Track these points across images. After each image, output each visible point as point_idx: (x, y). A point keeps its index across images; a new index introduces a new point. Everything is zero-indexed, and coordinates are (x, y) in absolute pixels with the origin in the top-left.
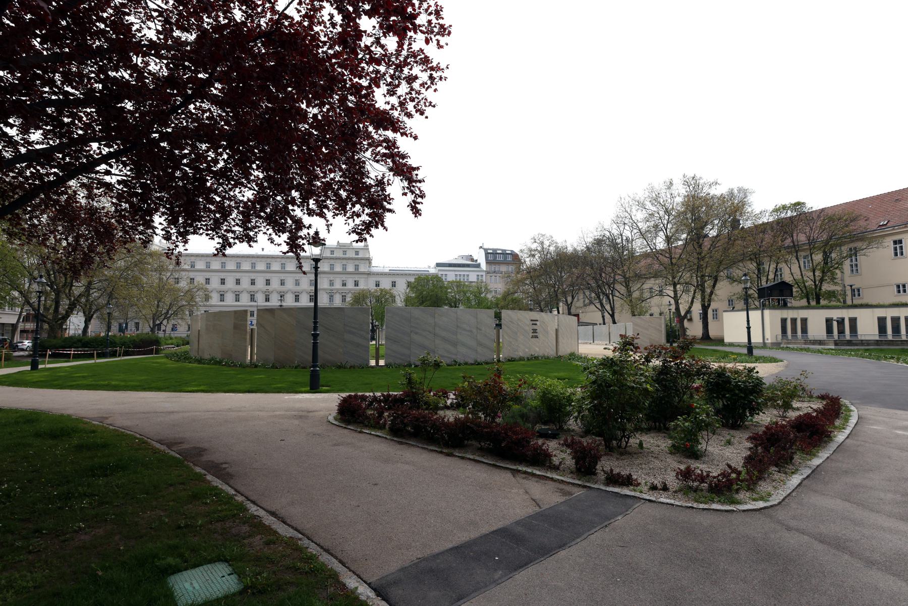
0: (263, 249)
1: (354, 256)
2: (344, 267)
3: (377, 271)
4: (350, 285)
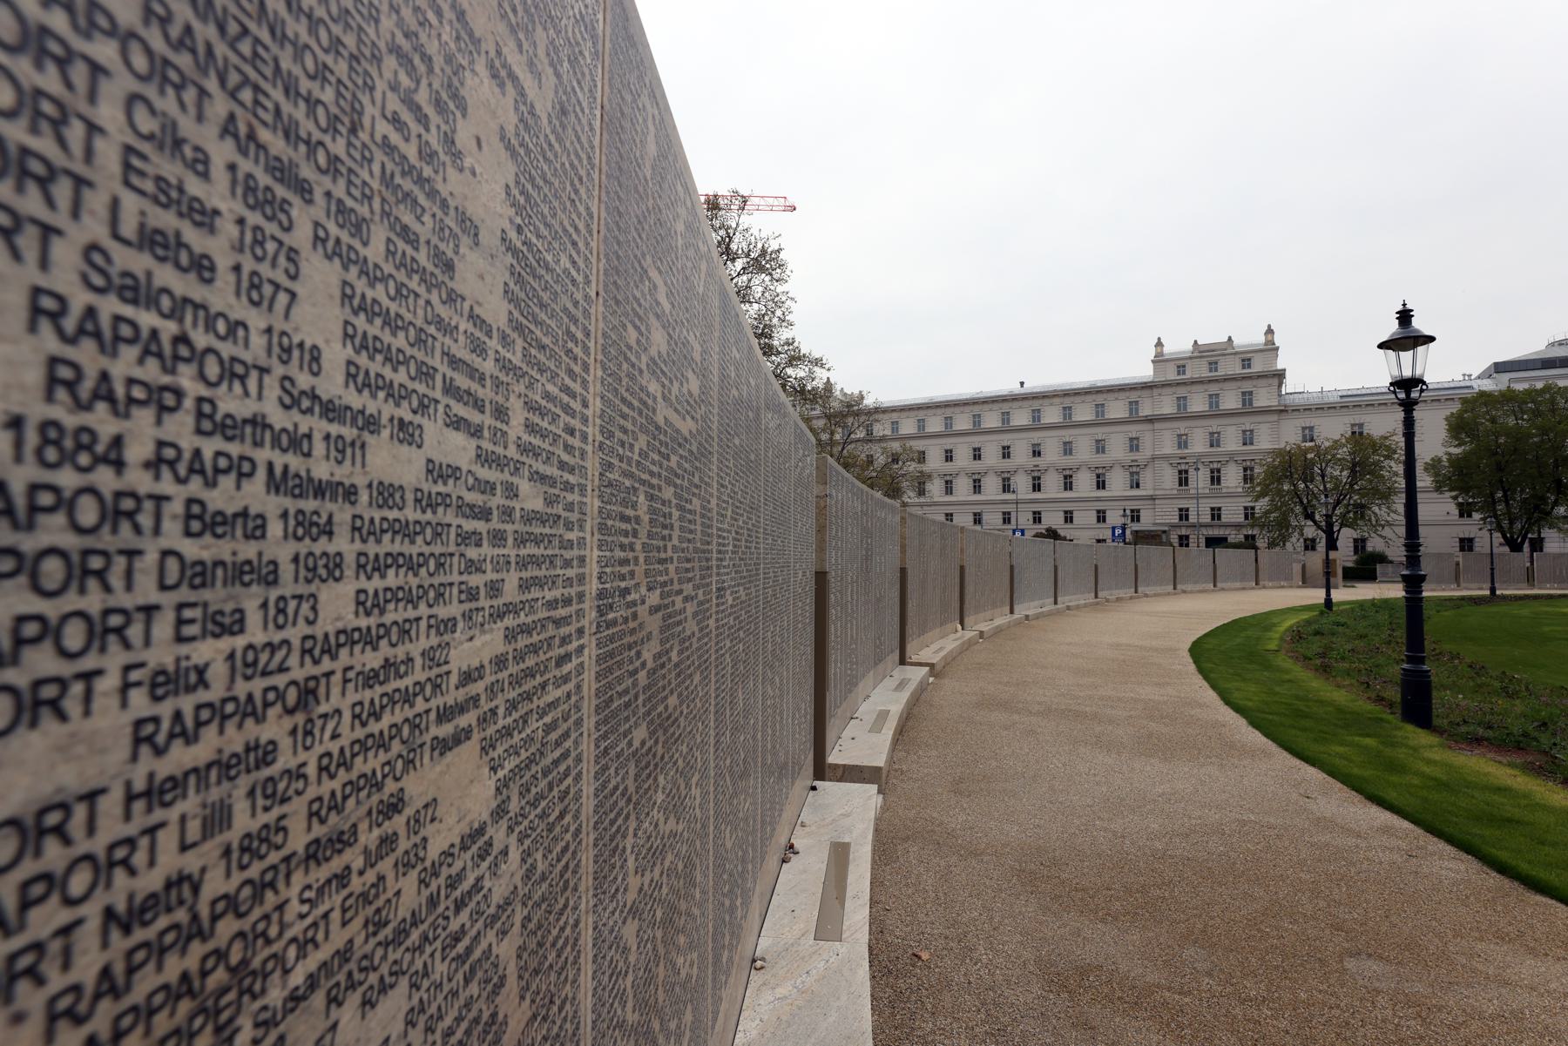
0: (1022, 384)
1: (1237, 369)
2: (1214, 399)
3: (1302, 402)
4: (1232, 442)
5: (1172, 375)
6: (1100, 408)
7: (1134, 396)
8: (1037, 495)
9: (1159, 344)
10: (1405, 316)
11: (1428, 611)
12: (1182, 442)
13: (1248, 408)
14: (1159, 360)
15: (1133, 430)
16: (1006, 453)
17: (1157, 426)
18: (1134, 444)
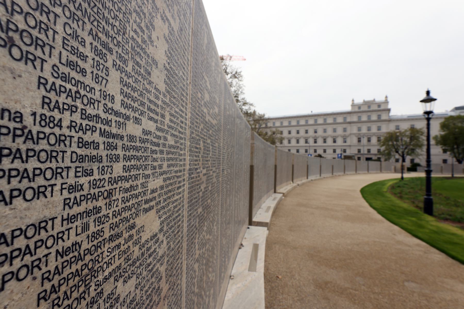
0: (312, 112)
2: (369, 117)
4: (374, 130)
5: (357, 110)
6: (335, 119)
7: (345, 116)
8: (315, 145)
9: (353, 100)
10: (428, 93)
11: (433, 181)
12: (359, 129)
13: (379, 120)
14: (353, 105)
15: (345, 126)
16: (307, 132)
17: (352, 124)
18: (345, 130)
